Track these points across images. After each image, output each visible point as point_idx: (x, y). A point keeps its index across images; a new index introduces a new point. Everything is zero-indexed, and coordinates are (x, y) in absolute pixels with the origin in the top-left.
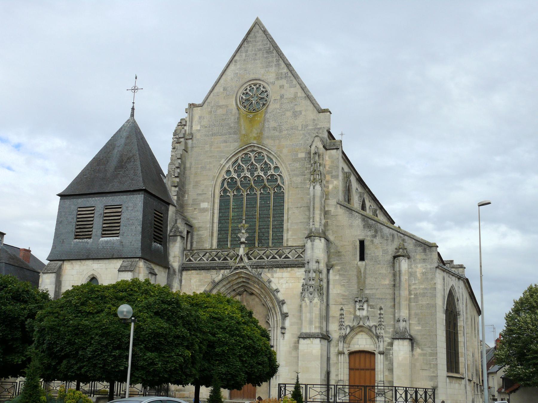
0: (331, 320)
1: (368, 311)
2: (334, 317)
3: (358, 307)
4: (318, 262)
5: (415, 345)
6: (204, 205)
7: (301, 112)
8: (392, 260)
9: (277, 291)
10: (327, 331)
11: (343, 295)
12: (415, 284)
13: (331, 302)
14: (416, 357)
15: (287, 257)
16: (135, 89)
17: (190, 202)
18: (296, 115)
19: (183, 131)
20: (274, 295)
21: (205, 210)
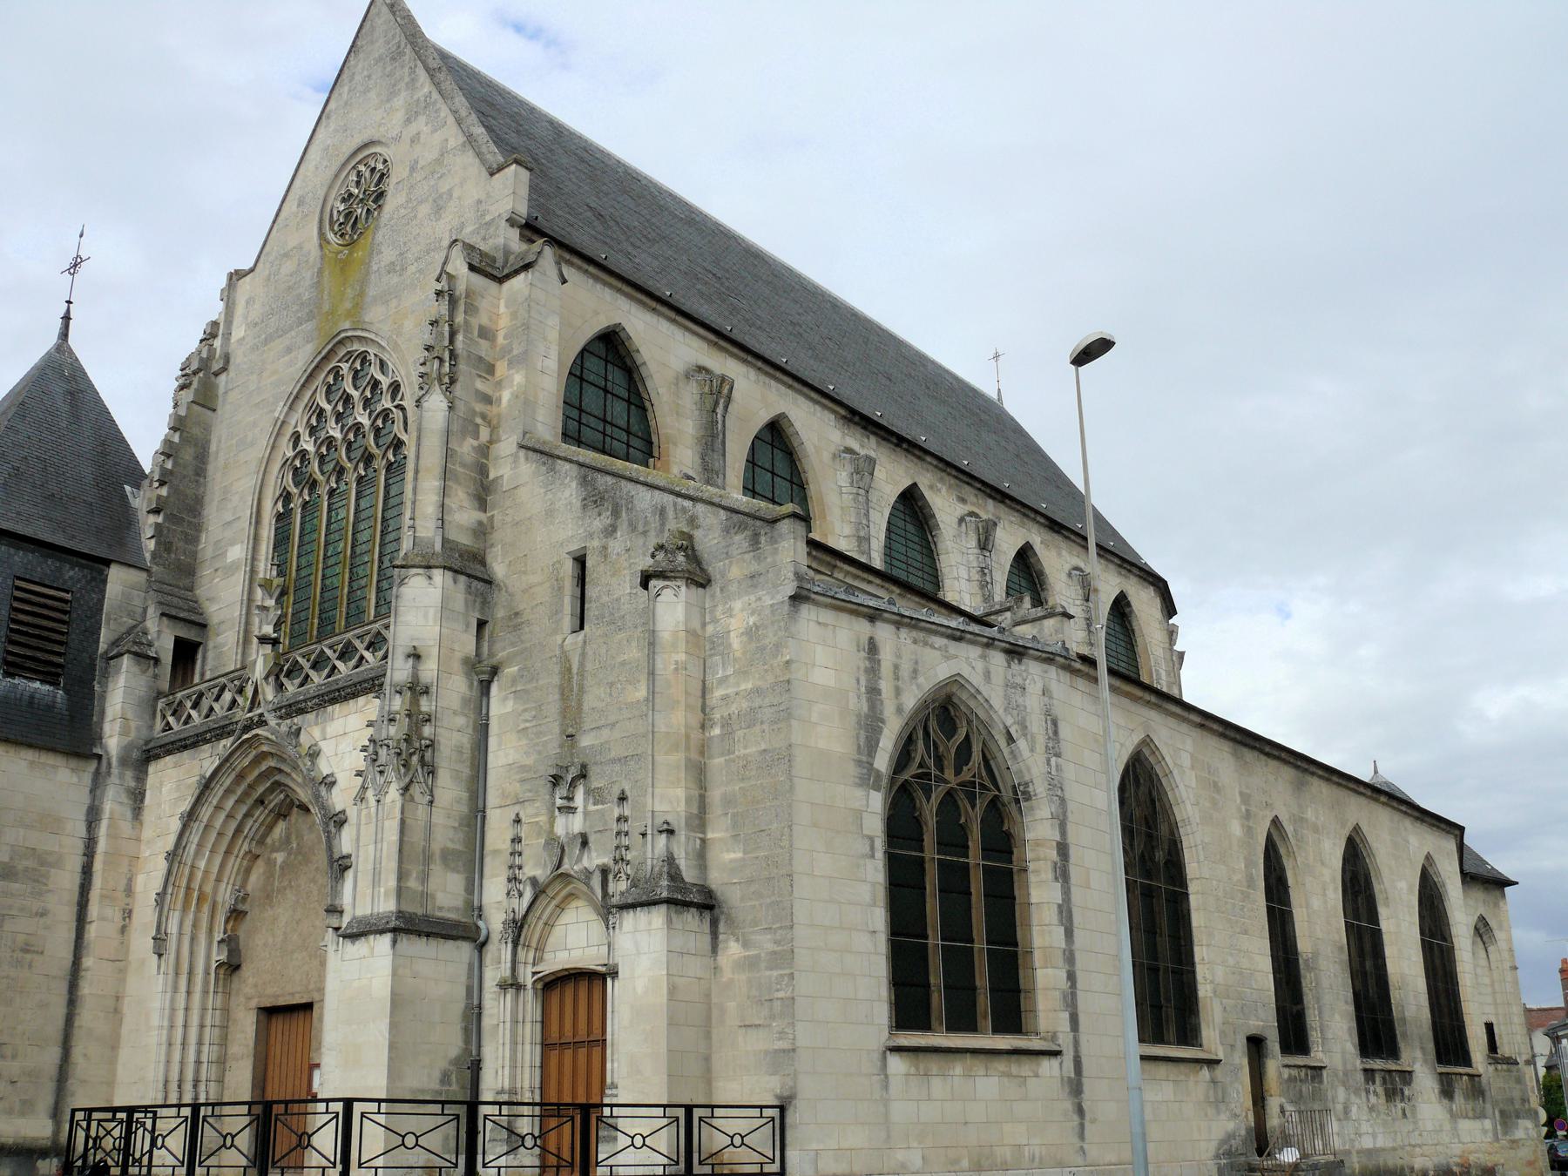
1: (586, 813)
2: (496, 852)
4: (416, 656)
5: (722, 927)
7: (450, 193)
11: (523, 768)
12: (725, 679)
14: (727, 974)
20: (317, 796)
21: (233, 568)
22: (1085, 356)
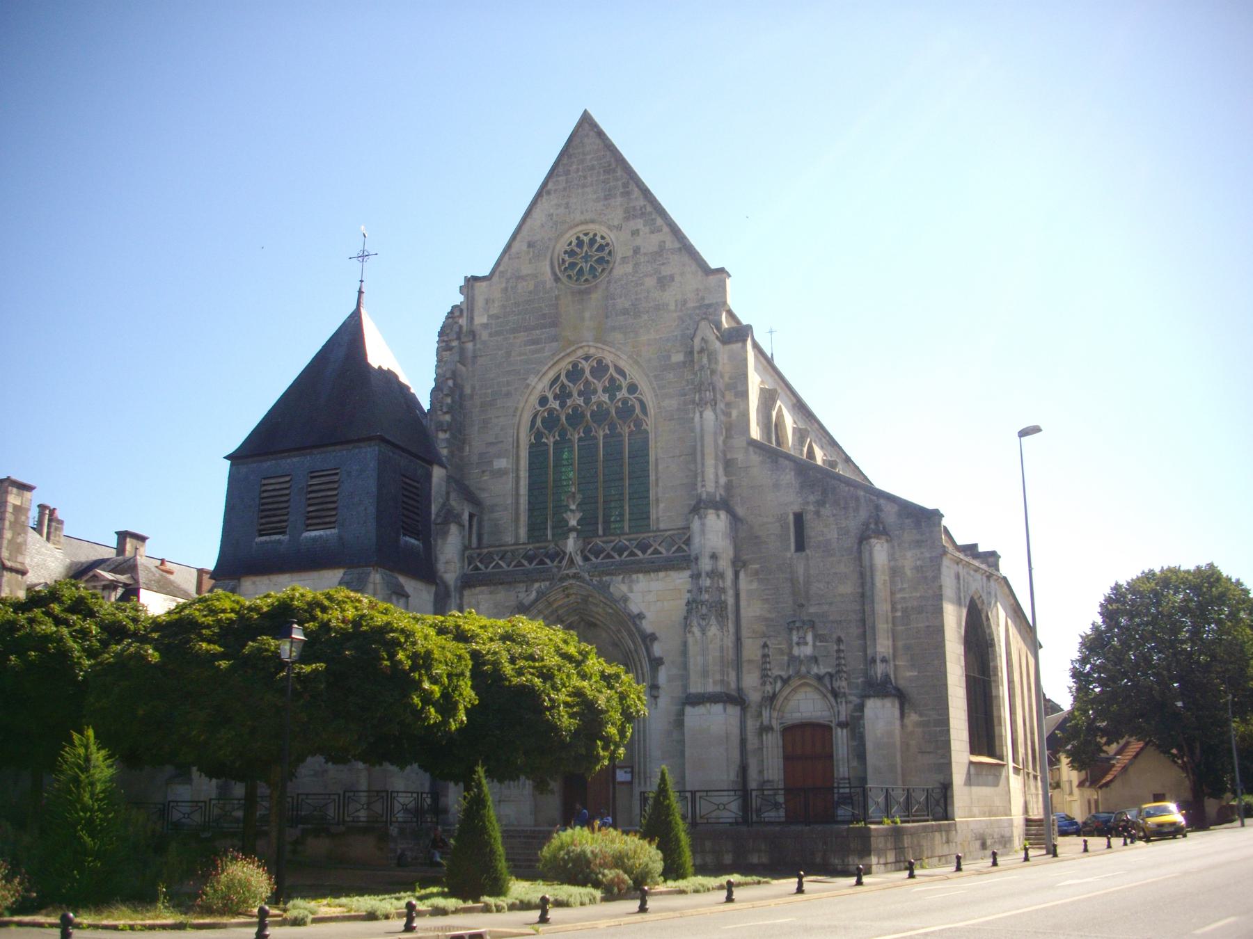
0: (745, 668)
1: (814, 646)
2: (750, 661)
3: (795, 638)
4: (714, 557)
5: (906, 706)
6: (501, 463)
7: (672, 278)
8: (856, 547)
9: (640, 616)
10: (739, 689)
11: (766, 619)
12: (901, 590)
13: (745, 633)
14: (910, 728)
15: (656, 552)
16: (363, 256)
17: (475, 459)
18: (664, 282)
19: (456, 328)
20: (635, 624)
21: (502, 473)
22: (1024, 433)
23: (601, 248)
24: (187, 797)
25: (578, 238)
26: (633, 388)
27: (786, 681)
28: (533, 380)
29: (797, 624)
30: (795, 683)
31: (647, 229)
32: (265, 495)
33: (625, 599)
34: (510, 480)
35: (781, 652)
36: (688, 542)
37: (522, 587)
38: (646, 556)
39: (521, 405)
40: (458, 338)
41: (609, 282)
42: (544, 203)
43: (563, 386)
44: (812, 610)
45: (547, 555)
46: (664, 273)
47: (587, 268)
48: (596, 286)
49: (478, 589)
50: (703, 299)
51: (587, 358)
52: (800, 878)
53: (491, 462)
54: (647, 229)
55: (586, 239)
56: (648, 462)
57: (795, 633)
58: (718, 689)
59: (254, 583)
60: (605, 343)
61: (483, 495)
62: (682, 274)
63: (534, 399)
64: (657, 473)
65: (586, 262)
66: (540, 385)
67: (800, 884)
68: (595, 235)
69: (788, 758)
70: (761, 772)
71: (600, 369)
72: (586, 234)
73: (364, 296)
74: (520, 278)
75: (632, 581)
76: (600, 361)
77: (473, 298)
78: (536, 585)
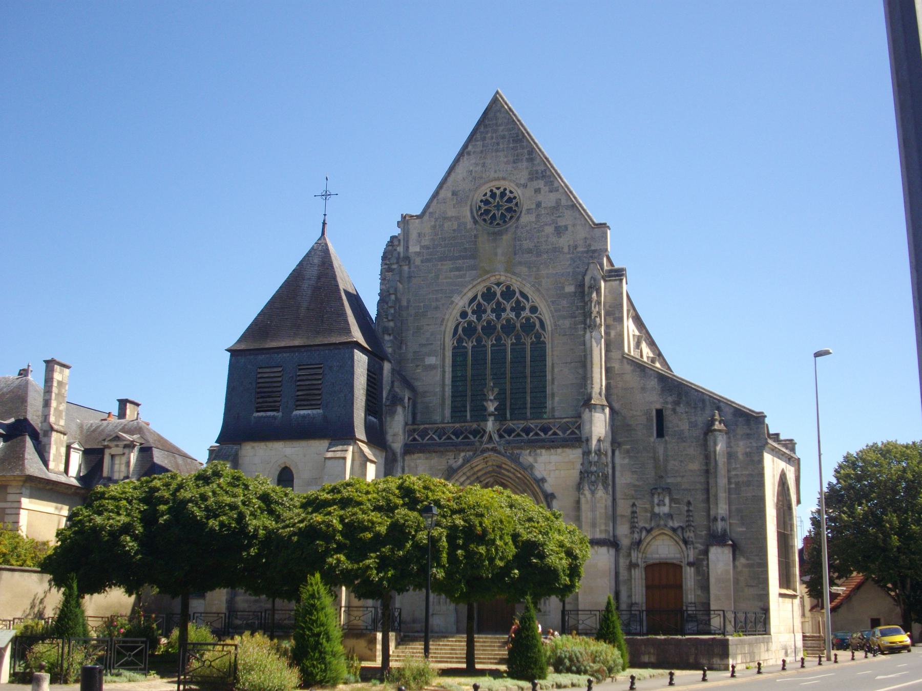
0: (619, 519)
1: (670, 507)
2: (622, 516)
3: (656, 501)
5: (737, 552)
6: (431, 360)
7: (566, 228)
8: (702, 436)
9: (543, 480)
10: (614, 536)
11: (635, 486)
12: (735, 469)
13: (619, 495)
14: (740, 568)
15: (555, 434)
16: (326, 195)
17: (410, 356)
18: (559, 231)
19: (395, 254)
21: (433, 367)
22: (818, 355)
23: (510, 200)
24: (201, 609)
25: (491, 191)
26: (534, 309)
27: (649, 531)
28: (456, 299)
29: (659, 491)
30: (655, 532)
31: (547, 189)
32: (260, 380)
33: (531, 467)
34: (439, 372)
35: (646, 510)
36: (579, 427)
37: (451, 455)
38: (547, 436)
39: (447, 317)
40: (397, 263)
41: (517, 227)
42: (465, 163)
43: (479, 305)
44: (669, 480)
45: (470, 433)
46: (560, 224)
47: (498, 215)
48: (507, 230)
49: (416, 455)
50: (590, 245)
51: (498, 284)
52: (705, 671)
53: (423, 360)
54: (547, 189)
55: (498, 192)
56: (545, 365)
57: (656, 496)
58: (603, 536)
59: (253, 448)
60: (514, 274)
61: (417, 384)
62: (574, 225)
63: (456, 312)
64: (552, 375)
65: (498, 210)
66: (461, 302)
67: (704, 675)
68: (505, 189)
69: (649, 587)
70: (630, 596)
71: (508, 293)
72: (498, 188)
73: (327, 227)
74: (446, 219)
75: (536, 454)
76: (508, 287)
77: (408, 231)
78: (462, 454)
